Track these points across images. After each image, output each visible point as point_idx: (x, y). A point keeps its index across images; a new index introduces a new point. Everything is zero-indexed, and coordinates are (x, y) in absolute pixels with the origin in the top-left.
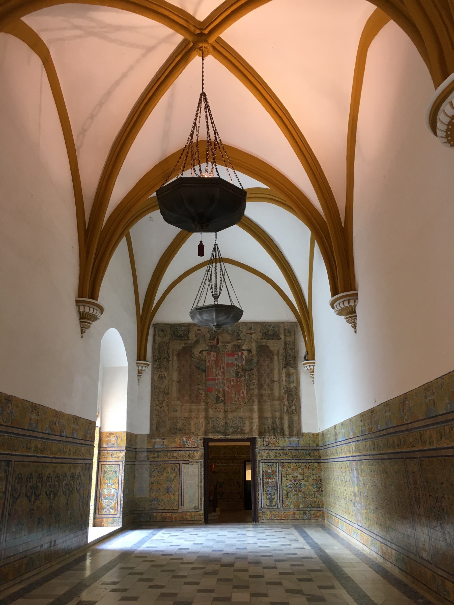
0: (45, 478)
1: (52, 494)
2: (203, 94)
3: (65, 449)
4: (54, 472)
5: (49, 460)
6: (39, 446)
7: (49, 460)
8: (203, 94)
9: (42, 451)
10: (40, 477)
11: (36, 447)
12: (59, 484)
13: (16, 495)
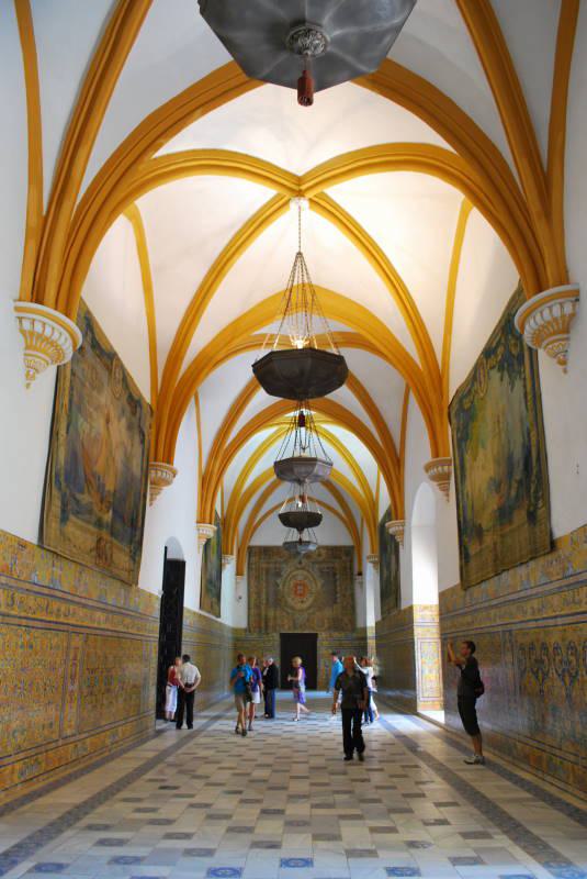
0: (551, 650)
1: (567, 674)
2: (299, 254)
3: (577, 598)
4: (563, 640)
5: (551, 622)
6: (536, 606)
7: (551, 622)
8: (299, 254)
9: (539, 610)
10: (544, 647)
11: (532, 608)
12: (577, 660)
13: (523, 668)
